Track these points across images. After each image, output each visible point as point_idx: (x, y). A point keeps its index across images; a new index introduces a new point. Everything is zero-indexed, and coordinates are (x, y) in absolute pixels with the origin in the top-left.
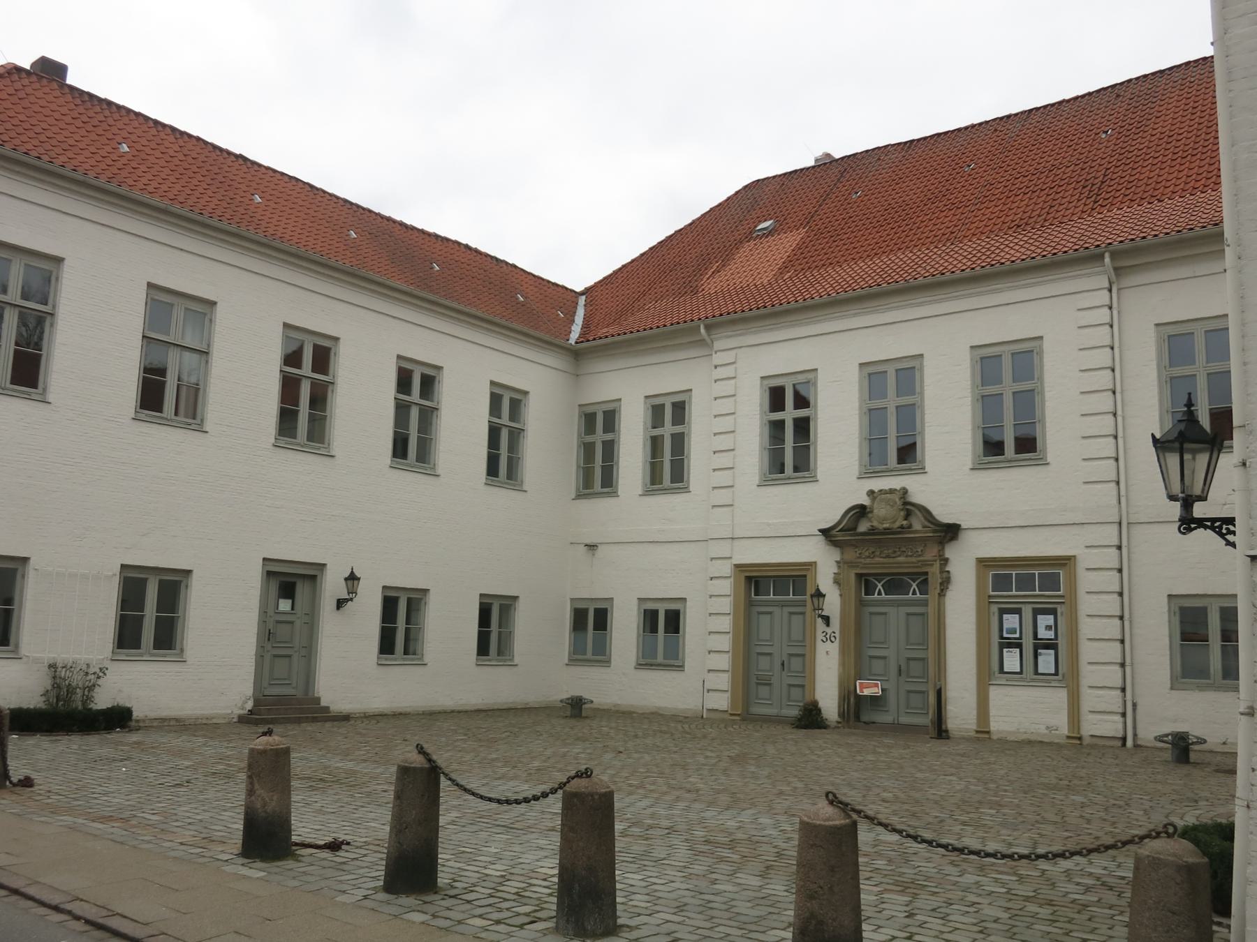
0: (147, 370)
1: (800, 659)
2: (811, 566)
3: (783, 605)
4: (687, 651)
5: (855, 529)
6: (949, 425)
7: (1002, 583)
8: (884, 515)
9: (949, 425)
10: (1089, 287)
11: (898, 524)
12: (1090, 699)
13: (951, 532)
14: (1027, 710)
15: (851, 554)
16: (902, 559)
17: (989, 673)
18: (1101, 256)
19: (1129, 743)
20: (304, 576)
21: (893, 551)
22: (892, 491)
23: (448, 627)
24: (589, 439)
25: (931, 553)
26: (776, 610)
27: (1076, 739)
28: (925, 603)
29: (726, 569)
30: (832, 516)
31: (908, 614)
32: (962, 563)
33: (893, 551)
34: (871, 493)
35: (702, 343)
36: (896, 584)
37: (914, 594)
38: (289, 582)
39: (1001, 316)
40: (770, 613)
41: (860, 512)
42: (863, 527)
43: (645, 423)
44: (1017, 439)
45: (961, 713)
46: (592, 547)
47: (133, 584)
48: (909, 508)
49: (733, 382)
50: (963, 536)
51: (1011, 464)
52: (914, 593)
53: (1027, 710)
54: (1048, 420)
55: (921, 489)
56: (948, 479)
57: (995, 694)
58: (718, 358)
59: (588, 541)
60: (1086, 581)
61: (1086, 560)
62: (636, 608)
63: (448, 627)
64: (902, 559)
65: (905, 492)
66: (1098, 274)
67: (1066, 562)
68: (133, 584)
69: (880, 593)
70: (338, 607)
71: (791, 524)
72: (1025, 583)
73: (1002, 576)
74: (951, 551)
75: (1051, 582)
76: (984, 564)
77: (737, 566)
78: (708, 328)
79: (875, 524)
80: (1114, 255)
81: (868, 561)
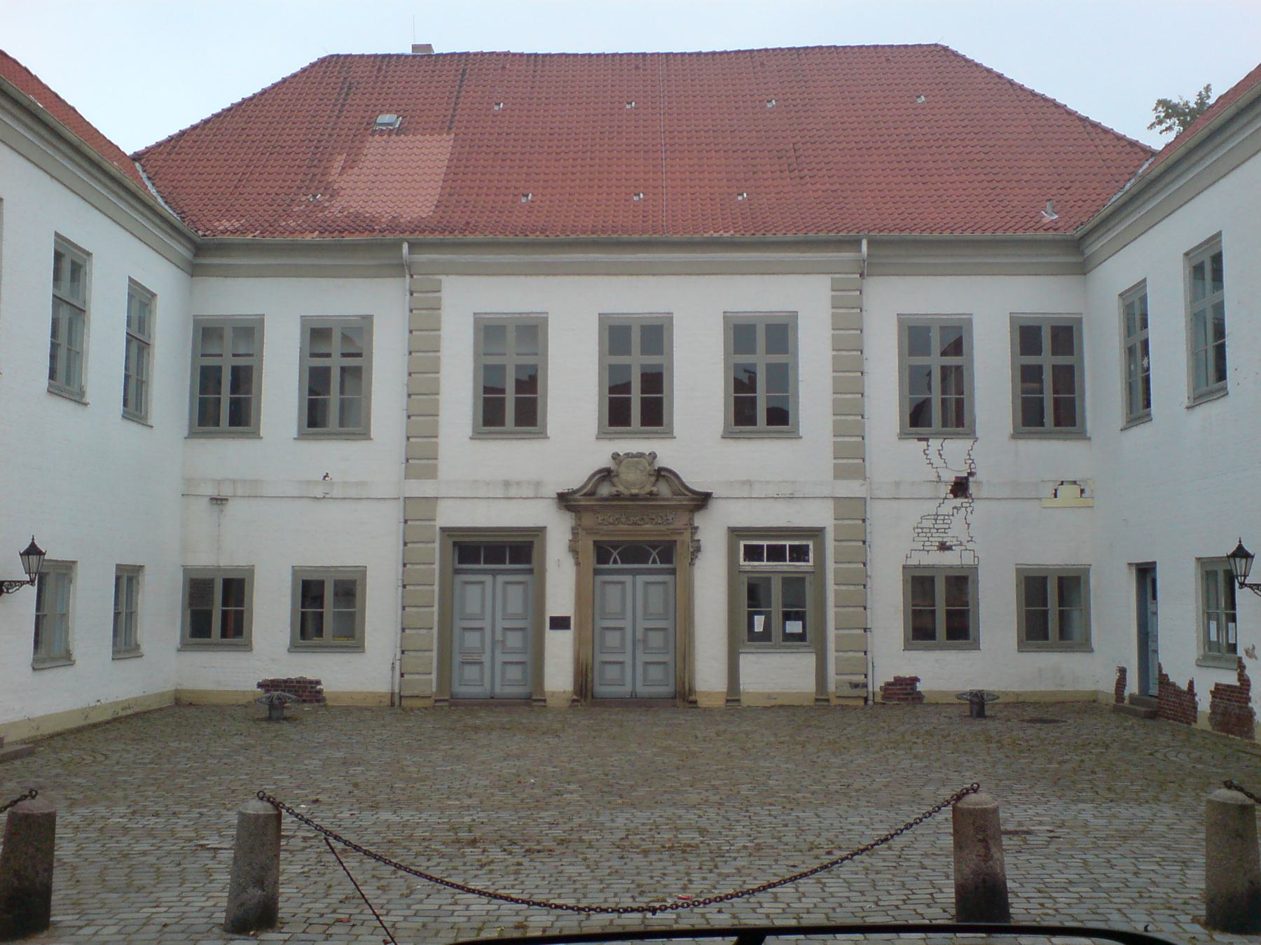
2: (540, 531)
3: (494, 573)
8: (632, 482)
11: (648, 489)
13: (702, 500)
14: (778, 674)
15: (588, 520)
16: (647, 527)
22: (641, 455)
25: (680, 521)
27: (822, 699)
28: (673, 572)
30: (575, 477)
32: (712, 532)
34: (615, 456)
36: (634, 553)
40: (482, 583)
41: (606, 475)
42: (605, 490)
48: (662, 474)
51: (761, 435)
55: (667, 452)
56: (695, 444)
64: (647, 527)
65: (653, 456)
71: (521, 481)
72: (776, 554)
73: (754, 545)
74: (699, 520)
76: (736, 533)
78: (412, 246)
81: (611, 527)
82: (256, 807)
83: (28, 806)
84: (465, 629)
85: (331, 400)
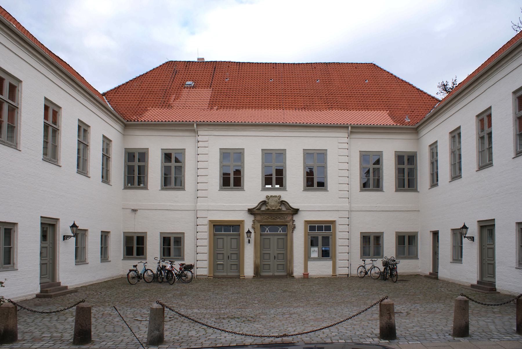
0: (224, 174)
1: (222, 255)
2: (242, 222)
4: (185, 253)
5: (260, 209)
6: (295, 175)
7: (312, 228)
9: (295, 175)
10: (342, 136)
11: (278, 208)
12: (339, 263)
13: (296, 211)
14: (320, 268)
15: (258, 218)
16: (278, 220)
17: (307, 257)
18: (348, 127)
19: (349, 276)
20: (50, 225)
21: (274, 218)
22: (275, 196)
23: (153, 247)
24: (131, 164)
25: (289, 218)
26: (271, 237)
27: (334, 275)
28: (286, 235)
29: (206, 222)
30: (253, 204)
31: (278, 239)
32: (299, 222)
33: (274, 218)
34: (267, 197)
35: (194, 131)
37: (280, 231)
38: (48, 227)
39: (315, 141)
40: (223, 238)
41: (264, 203)
42: (263, 208)
43: (162, 160)
44: (318, 182)
45: (298, 271)
46: (135, 211)
47: (366, 238)
48: (283, 203)
49: (207, 148)
50: (299, 213)
51: (316, 190)
52: (267, 231)
53: (320, 268)
54: (328, 177)
55: (285, 196)
56: (294, 192)
57: (310, 263)
58: (200, 138)
59: (133, 208)
60: (339, 228)
61: (339, 221)
62: (159, 237)
63: (153, 247)
64: (278, 220)
65: (280, 197)
66: (345, 132)
67: (333, 222)
68: (366, 238)
69: (267, 231)
70: (64, 239)
71: (235, 207)
72: (320, 228)
73: (312, 226)
74: (295, 218)
75: (328, 228)
76: (307, 222)
77: (210, 221)
79: (269, 207)
80: (352, 127)
81: (266, 220)
82: (155, 306)
83: (82, 305)
84: (218, 254)
85: (173, 178)
